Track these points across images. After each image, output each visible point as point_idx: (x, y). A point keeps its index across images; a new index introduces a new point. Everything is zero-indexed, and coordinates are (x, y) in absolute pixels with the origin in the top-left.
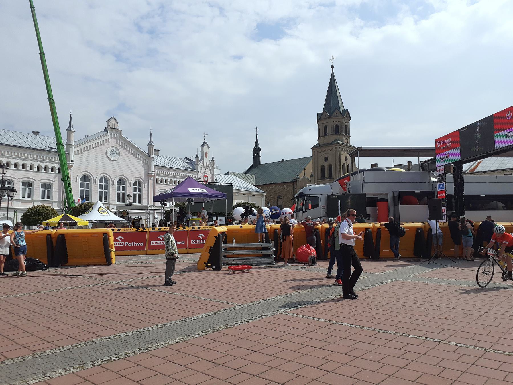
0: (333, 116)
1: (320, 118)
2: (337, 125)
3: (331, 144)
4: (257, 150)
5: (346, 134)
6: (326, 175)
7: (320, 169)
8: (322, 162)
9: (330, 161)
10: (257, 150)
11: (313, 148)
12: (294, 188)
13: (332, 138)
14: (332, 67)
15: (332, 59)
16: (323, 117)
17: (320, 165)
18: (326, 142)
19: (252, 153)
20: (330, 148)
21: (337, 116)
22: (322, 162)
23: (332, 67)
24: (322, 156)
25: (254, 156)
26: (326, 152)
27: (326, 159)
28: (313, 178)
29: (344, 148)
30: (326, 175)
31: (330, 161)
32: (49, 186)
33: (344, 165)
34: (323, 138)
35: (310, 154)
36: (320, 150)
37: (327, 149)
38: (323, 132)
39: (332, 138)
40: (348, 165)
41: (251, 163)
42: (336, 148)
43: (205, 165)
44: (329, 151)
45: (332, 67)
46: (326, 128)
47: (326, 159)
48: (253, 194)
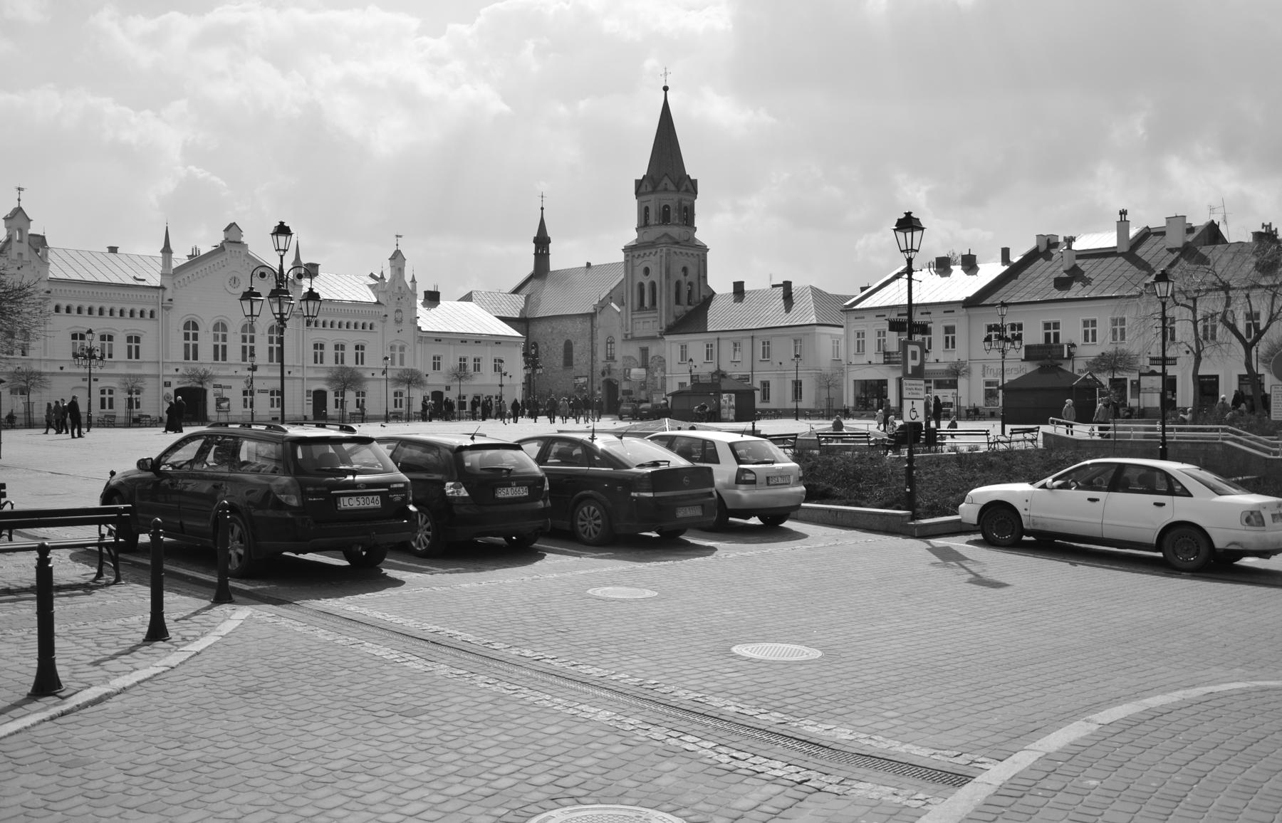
1: (641, 188)
2: (666, 206)
3: (652, 244)
4: (542, 242)
6: (647, 303)
7: (636, 289)
8: (640, 277)
10: (542, 242)
11: (628, 250)
13: (655, 232)
16: (643, 189)
17: (636, 283)
19: (532, 248)
20: (653, 251)
21: (666, 190)
22: (640, 277)
25: (536, 254)
27: (647, 271)
30: (647, 303)
33: (678, 284)
35: (620, 257)
37: (647, 252)
39: (655, 232)
41: (530, 269)
43: (396, 290)
46: (647, 209)
47: (647, 271)
48: (497, 341)
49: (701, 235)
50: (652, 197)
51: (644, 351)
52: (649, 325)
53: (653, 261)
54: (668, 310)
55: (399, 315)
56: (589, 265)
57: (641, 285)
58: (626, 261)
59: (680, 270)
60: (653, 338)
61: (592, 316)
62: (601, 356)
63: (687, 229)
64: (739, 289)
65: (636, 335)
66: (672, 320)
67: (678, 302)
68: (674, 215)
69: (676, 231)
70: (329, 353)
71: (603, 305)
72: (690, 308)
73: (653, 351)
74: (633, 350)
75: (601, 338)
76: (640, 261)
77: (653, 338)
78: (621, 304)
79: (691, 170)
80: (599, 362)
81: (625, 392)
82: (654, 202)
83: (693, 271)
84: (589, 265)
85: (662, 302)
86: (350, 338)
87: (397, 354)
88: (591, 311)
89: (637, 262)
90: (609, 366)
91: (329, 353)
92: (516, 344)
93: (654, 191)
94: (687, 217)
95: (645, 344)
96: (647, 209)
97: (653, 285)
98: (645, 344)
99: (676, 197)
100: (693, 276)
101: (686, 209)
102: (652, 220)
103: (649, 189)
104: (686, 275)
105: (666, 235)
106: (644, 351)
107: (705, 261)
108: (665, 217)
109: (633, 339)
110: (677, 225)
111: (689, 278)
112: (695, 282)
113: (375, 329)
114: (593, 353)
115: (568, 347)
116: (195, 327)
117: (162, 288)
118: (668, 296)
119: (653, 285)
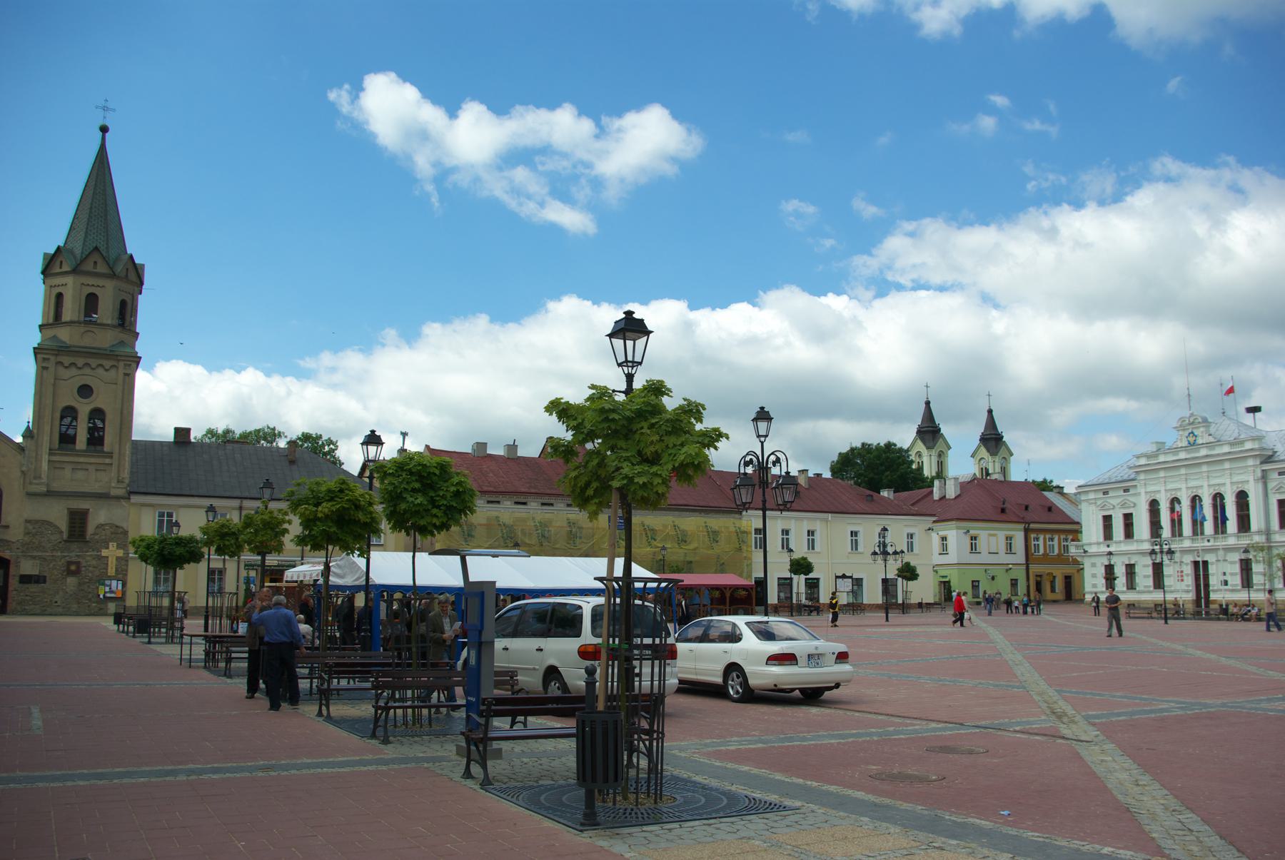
1: (50, 266)
9: (98, 401)
14: (104, 130)
20: (107, 363)
26: (87, 371)
27: (85, 391)
36: (67, 360)
37: (94, 362)
44: (100, 371)
45: (104, 130)
57: (70, 412)
60: (104, 496)
63: (123, 336)
73: (100, 516)
74: (57, 514)
76: (73, 371)
77: (104, 496)
79: (136, 245)
81: (26, 579)
82: (71, 288)
93: (75, 271)
96: (60, 296)
119: (97, 414)
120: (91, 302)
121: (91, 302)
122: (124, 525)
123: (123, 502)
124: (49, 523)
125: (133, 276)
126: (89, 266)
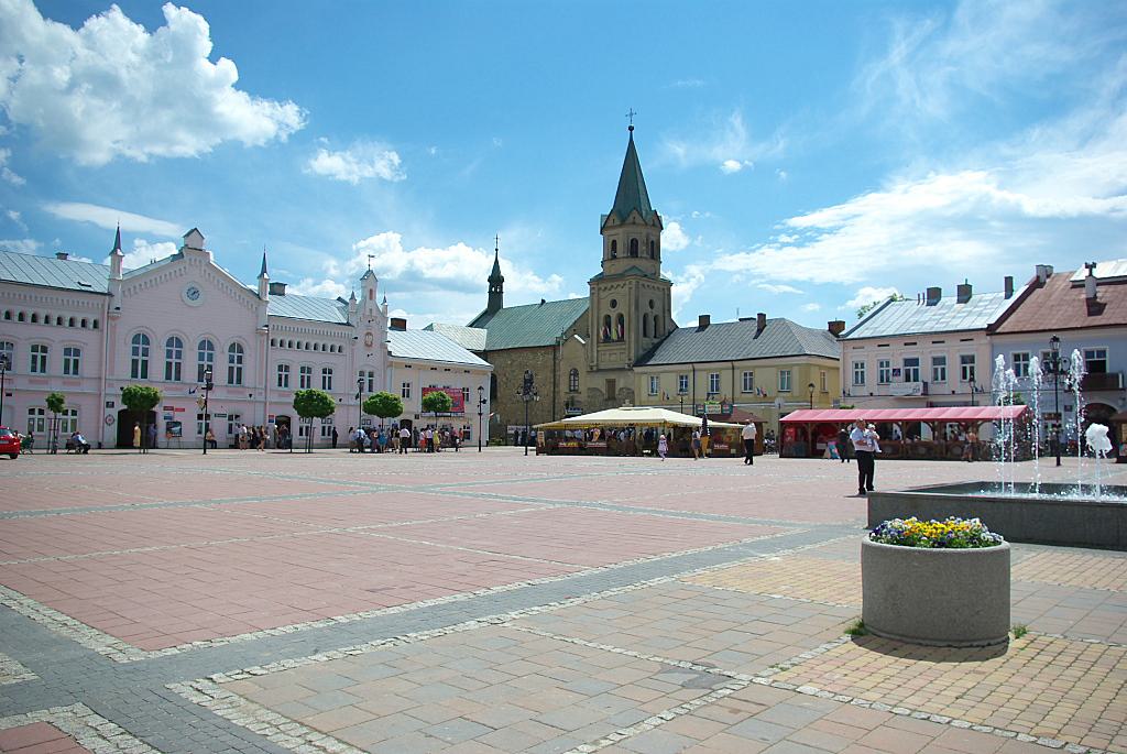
0: (627, 222)
3: (621, 276)
4: (496, 280)
5: (652, 258)
7: (602, 322)
8: (606, 310)
9: (622, 308)
10: (496, 280)
11: (595, 282)
12: (554, 358)
13: (622, 265)
14: (631, 129)
15: (631, 114)
16: (610, 223)
17: (602, 316)
18: (613, 272)
20: (621, 283)
21: (634, 223)
23: (631, 129)
24: (607, 297)
26: (613, 290)
27: (614, 304)
28: (589, 340)
29: (646, 284)
31: (622, 308)
32: (972, 359)
34: (607, 264)
36: (602, 286)
37: (615, 284)
38: (612, 251)
39: (622, 265)
40: (655, 318)
41: (485, 306)
42: (630, 283)
43: (368, 313)
44: (619, 289)
46: (614, 242)
47: (614, 304)
48: (467, 370)
49: (665, 273)
50: (620, 230)
51: (611, 384)
52: (616, 356)
53: (622, 293)
54: (637, 341)
55: (369, 338)
56: (543, 301)
58: (592, 294)
59: (648, 303)
61: (554, 348)
62: (563, 387)
64: (704, 321)
65: (602, 367)
66: (641, 352)
67: (645, 335)
68: (642, 248)
69: (643, 264)
70: (295, 377)
71: (568, 335)
72: (656, 341)
73: (620, 384)
75: (564, 369)
78: (586, 336)
80: (562, 394)
83: (658, 304)
84: (543, 301)
85: (631, 337)
86: (318, 361)
87: (367, 379)
88: (551, 341)
89: (603, 294)
90: (572, 398)
91: (295, 377)
92: (485, 373)
93: (620, 226)
94: (654, 251)
95: (612, 376)
96: (614, 242)
97: (621, 319)
98: (612, 376)
99: (644, 231)
100: (657, 310)
101: (652, 242)
102: (619, 253)
103: (618, 222)
104: (652, 307)
105: (634, 267)
106: (611, 384)
107: (669, 295)
108: (633, 249)
109: (599, 370)
110: (646, 258)
111: (655, 313)
112: (661, 315)
113: (344, 352)
114: (555, 385)
115: (528, 382)
116: (179, 344)
117: (109, 294)
118: (638, 328)
119: (621, 319)
120: (634, 243)
121: (634, 243)
122: (632, 387)
123: (629, 373)
124: (598, 389)
125: (656, 221)
126: (631, 219)
